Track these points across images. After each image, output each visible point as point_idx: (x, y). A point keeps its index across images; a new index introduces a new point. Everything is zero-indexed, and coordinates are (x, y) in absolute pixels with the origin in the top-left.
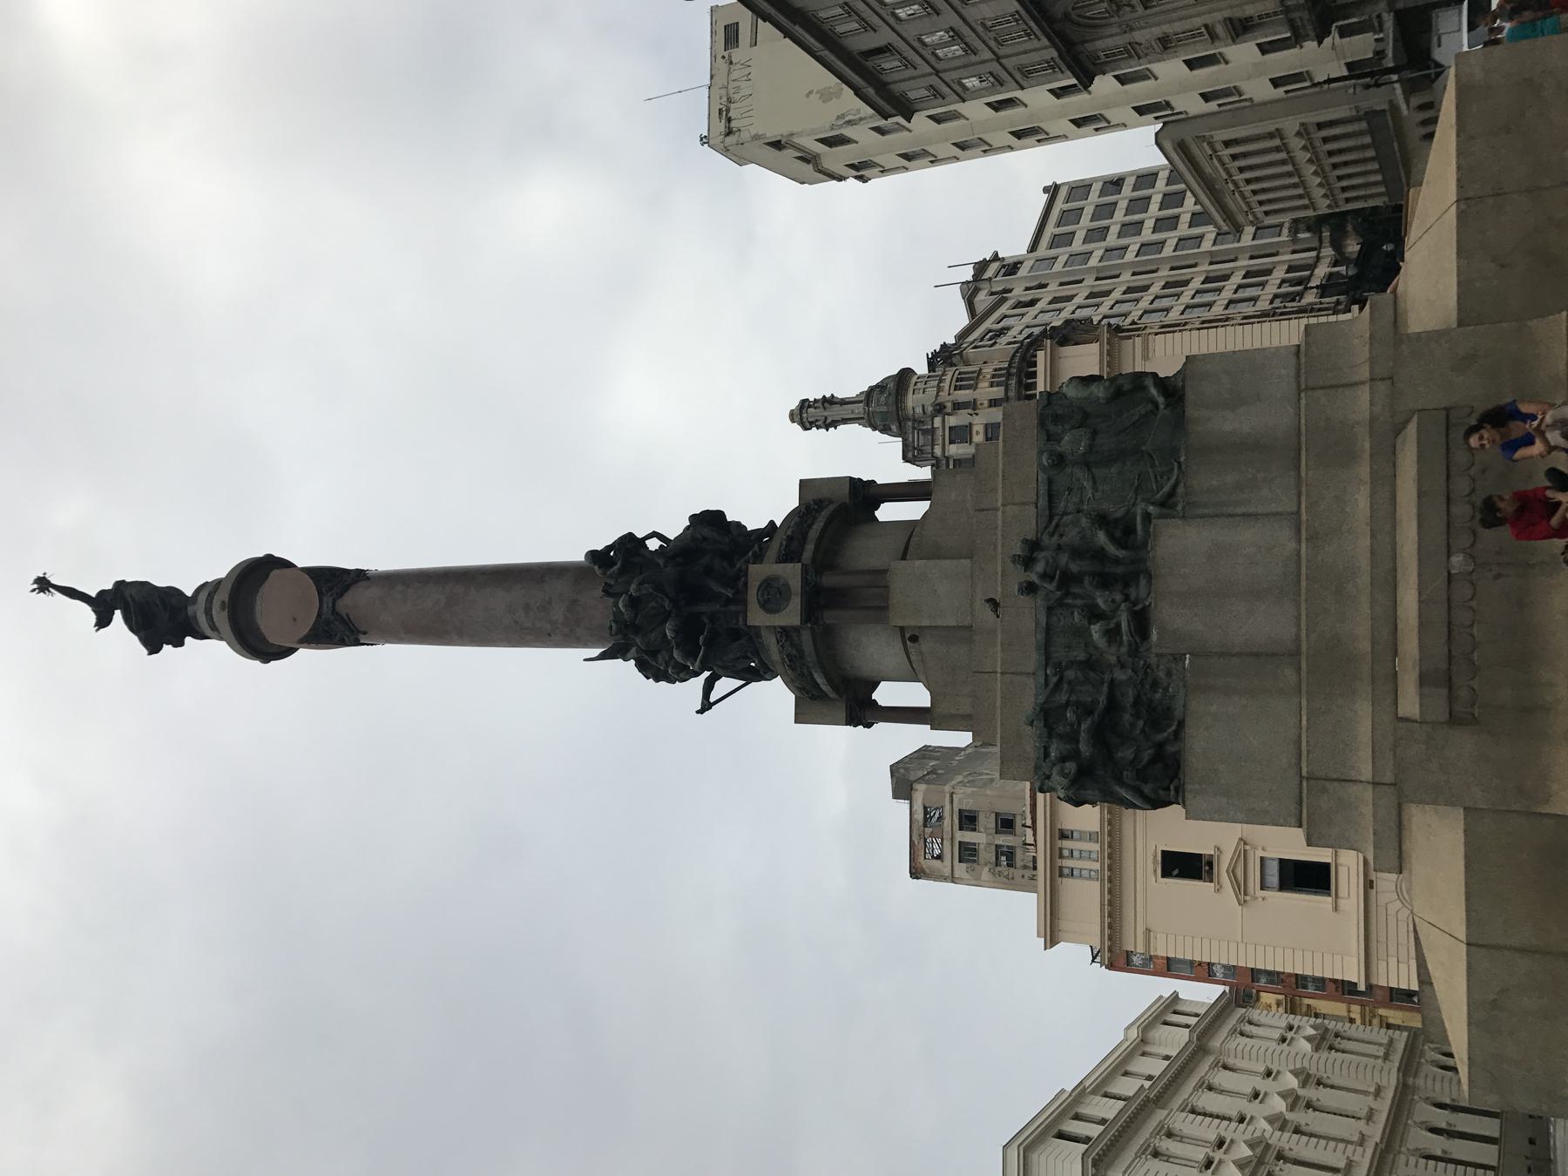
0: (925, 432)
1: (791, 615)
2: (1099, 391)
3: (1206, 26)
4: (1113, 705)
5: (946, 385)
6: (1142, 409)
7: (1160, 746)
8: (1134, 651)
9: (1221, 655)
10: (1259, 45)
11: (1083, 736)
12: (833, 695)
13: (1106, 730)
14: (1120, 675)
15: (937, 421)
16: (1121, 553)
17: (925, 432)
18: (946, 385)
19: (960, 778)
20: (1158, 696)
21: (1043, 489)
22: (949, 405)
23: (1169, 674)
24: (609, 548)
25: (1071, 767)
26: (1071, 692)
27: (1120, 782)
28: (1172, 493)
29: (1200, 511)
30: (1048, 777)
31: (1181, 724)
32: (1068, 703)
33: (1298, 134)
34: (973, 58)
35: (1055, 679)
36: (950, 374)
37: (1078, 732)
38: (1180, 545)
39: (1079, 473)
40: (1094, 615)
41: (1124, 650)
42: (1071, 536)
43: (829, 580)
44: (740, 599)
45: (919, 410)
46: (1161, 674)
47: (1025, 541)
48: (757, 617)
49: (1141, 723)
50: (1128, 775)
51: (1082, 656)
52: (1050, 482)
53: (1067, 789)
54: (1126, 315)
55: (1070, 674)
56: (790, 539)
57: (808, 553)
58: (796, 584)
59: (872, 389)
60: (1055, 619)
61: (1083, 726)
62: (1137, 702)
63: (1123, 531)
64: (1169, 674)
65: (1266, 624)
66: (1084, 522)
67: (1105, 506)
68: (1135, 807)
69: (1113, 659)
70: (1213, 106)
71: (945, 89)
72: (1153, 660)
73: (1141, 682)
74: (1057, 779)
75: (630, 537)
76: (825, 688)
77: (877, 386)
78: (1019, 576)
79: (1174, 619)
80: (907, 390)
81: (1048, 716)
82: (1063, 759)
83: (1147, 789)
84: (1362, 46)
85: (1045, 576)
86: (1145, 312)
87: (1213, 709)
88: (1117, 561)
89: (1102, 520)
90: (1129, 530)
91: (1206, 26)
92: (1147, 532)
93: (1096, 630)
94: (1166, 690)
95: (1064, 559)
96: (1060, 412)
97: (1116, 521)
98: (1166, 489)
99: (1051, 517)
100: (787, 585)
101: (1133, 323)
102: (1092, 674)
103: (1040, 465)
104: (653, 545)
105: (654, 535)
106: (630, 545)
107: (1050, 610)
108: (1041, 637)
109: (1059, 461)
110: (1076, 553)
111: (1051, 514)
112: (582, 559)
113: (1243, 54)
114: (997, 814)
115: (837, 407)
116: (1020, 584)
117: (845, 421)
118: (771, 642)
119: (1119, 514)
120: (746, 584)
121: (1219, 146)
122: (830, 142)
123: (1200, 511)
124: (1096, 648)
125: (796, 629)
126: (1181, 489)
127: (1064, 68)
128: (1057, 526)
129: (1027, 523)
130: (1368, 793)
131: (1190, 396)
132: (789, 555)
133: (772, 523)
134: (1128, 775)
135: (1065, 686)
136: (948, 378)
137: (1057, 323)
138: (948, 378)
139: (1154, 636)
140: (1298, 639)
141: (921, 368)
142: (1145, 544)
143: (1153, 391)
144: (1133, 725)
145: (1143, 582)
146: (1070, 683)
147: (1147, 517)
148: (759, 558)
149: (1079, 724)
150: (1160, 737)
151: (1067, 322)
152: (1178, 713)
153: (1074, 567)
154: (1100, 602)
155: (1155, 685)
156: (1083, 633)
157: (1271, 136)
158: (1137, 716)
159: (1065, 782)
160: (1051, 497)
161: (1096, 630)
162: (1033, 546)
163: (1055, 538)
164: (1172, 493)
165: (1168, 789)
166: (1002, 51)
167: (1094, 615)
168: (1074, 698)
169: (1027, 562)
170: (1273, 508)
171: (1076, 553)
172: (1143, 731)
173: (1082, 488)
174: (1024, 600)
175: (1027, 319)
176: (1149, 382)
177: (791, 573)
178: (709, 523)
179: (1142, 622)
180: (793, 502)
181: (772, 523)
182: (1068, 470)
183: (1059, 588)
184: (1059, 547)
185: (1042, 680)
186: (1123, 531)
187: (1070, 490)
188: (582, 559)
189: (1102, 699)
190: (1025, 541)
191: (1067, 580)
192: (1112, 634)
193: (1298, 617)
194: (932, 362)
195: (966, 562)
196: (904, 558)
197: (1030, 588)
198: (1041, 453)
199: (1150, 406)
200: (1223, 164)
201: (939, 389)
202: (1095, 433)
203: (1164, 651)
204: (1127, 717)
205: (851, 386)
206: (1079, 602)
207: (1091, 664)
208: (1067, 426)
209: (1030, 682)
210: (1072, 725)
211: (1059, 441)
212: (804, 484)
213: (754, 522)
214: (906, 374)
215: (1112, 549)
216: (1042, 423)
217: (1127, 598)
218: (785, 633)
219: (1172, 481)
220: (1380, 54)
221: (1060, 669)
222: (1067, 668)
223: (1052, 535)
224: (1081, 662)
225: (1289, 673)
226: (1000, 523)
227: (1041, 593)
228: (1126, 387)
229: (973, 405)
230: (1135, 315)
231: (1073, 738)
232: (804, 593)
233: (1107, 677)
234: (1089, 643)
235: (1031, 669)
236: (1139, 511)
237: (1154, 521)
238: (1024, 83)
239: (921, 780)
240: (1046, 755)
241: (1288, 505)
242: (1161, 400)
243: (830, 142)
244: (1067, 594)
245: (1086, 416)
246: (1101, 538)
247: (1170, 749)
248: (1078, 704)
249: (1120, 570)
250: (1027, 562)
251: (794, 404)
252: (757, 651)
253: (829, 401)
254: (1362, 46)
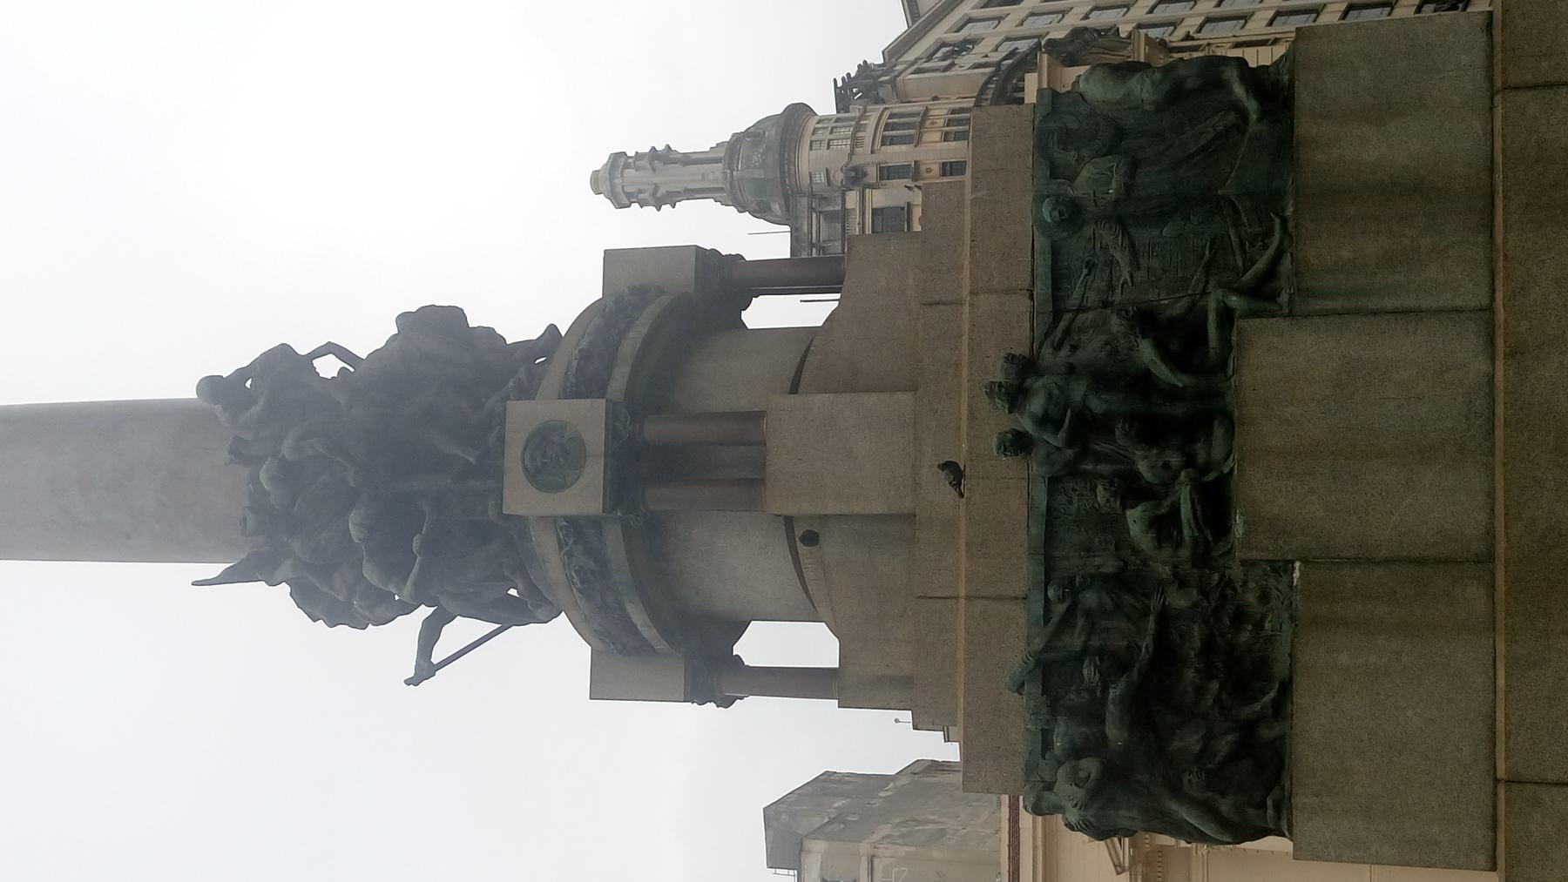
0: (831, 217)
1: (585, 495)
2: (1143, 89)
4: (1166, 654)
5: (867, 135)
6: (1219, 122)
7: (1248, 729)
8: (1203, 557)
9: (1356, 562)
11: (1112, 712)
12: (661, 645)
13: (1153, 702)
14: (1179, 601)
15: (852, 199)
16: (1180, 380)
17: (831, 217)
18: (867, 135)
19: (885, 829)
20: (1244, 637)
22: (873, 172)
23: (1264, 597)
24: (242, 374)
25: (1090, 767)
26: (1091, 630)
27: (1177, 792)
28: (1271, 273)
29: (1318, 305)
30: (1049, 787)
31: (1286, 688)
32: (1085, 651)
35: (1060, 609)
36: (874, 117)
37: (1103, 702)
38: (1283, 366)
39: (1107, 235)
40: (1131, 490)
41: (1185, 553)
42: (1092, 348)
43: (656, 430)
44: (490, 467)
45: (820, 179)
46: (1251, 598)
47: (1011, 358)
48: (522, 499)
49: (1214, 686)
51: (1110, 566)
52: (1055, 252)
53: (1085, 806)
54: (1174, 24)
56: (585, 356)
57: (618, 383)
58: (595, 438)
59: (738, 138)
60: (1062, 498)
61: (1114, 693)
62: (1208, 646)
63: (1183, 338)
64: (1264, 597)
66: (1116, 324)
67: (1152, 296)
68: (1202, 838)
69: (1165, 571)
72: (1236, 572)
73: (1216, 611)
74: (1065, 791)
75: (283, 353)
76: (649, 632)
77: (747, 133)
78: (999, 421)
80: (800, 140)
81: (1049, 674)
82: (1076, 753)
83: (1225, 806)
85: (1047, 421)
86: (1209, 20)
87: (1343, 658)
88: (1172, 394)
89: (1146, 321)
92: (1226, 346)
93: (1135, 519)
94: (1259, 626)
95: (1079, 390)
96: (1073, 126)
97: (1173, 322)
98: (1261, 265)
99: (1057, 315)
100: (578, 441)
101: (1188, 37)
102: (1128, 598)
103: (1039, 222)
104: (328, 367)
105: (330, 349)
106: (282, 368)
107: (1053, 483)
108: (1037, 530)
109: (1072, 215)
110: (1101, 379)
111: (1057, 312)
112: (191, 394)
115: (676, 169)
116: (1002, 436)
117: (691, 194)
118: (546, 544)
119: (1178, 309)
120: (502, 439)
123: (1318, 305)
124: (1136, 551)
125: (596, 523)
126: (1286, 265)
128: (1068, 331)
131: (1304, 97)
132: (583, 385)
133: (552, 329)
134: (1192, 781)
135: (1081, 622)
136: (870, 123)
137: (1059, 34)
138: (870, 123)
139: (1239, 529)
140: (1490, 533)
141: (825, 105)
142: (1223, 365)
143: (1239, 90)
144: (1200, 691)
145: (1218, 431)
146: (1088, 614)
148: (527, 391)
149: (1105, 689)
150: (1248, 711)
151: (1077, 33)
152: (1280, 668)
153: (1097, 405)
154: (1143, 467)
155: (1240, 617)
156: (1111, 524)
158: (1207, 673)
159: (1080, 794)
160: (1058, 278)
161: (1135, 519)
162: (1025, 368)
163: (1064, 352)
164: (1271, 273)
165: (1263, 806)
168: (1095, 642)
169: (1014, 395)
171: (1101, 379)
172: (1218, 700)
173: (1111, 263)
174: (1012, 466)
175: (1007, 27)
176: (1231, 74)
177: (588, 419)
178: (436, 333)
179: (1216, 502)
180: (592, 291)
181: (552, 329)
182: (1088, 230)
183: (1070, 443)
184: (1071, 370)
185: (1038, 609)
186: (1183, 338)
187: (1091, 266)
188: (191, 394)
189: (1146, 643)
190: (1011, 358)
192: (1165, 526)
193: (1491, 494)
194: (844, 93)
196: (794, 389)
197: (1018, 444)
198: (1039, 199)
199: (1232, 117)
201: (855, 142)
202: (1135, 165)
203: (1256, 555)
204: (1190, 675)
205: (702, 131)
206: (1104, 468)
207: (1128, 581)
208: (1085, 153)
209: (1018, 613)
210: (1092, 691)
211: (1071, 179)
212: (611, 258)
213: (519, 327)
214: (798, 113)
215: (1163, 372)
216: (1041, 147)
217: (1189, 462)
218: (575, 530)
219: (1271, 251)
221: (1072, 590)
222: (1084, 588)
223: (1058, 347)
224: (1106, 577)
225: (1474, 593)
226: (966, 327)
227: (1039, 453)
228: (1191, 84)
229: (912, 172)
230: (1191, 24)
231: (1094, 714)
233: (1155, 603)
234: (1122, 543)
235: (1020, 588)
236: (1212, 304)
237: (1239, 323)
239: (816, 833)
240: (1047, 745)
241: (1472, 295)
242: (1252, 106)
244: (1084, 453)
245: (1120, 134)
246: (1146, 352)
247: (1266, 733)
248: (1102, 652)
249: (1178, 409)
250: (1014, 395)
251: (600, 161)
252: (522, 565)
253: (662, 158)
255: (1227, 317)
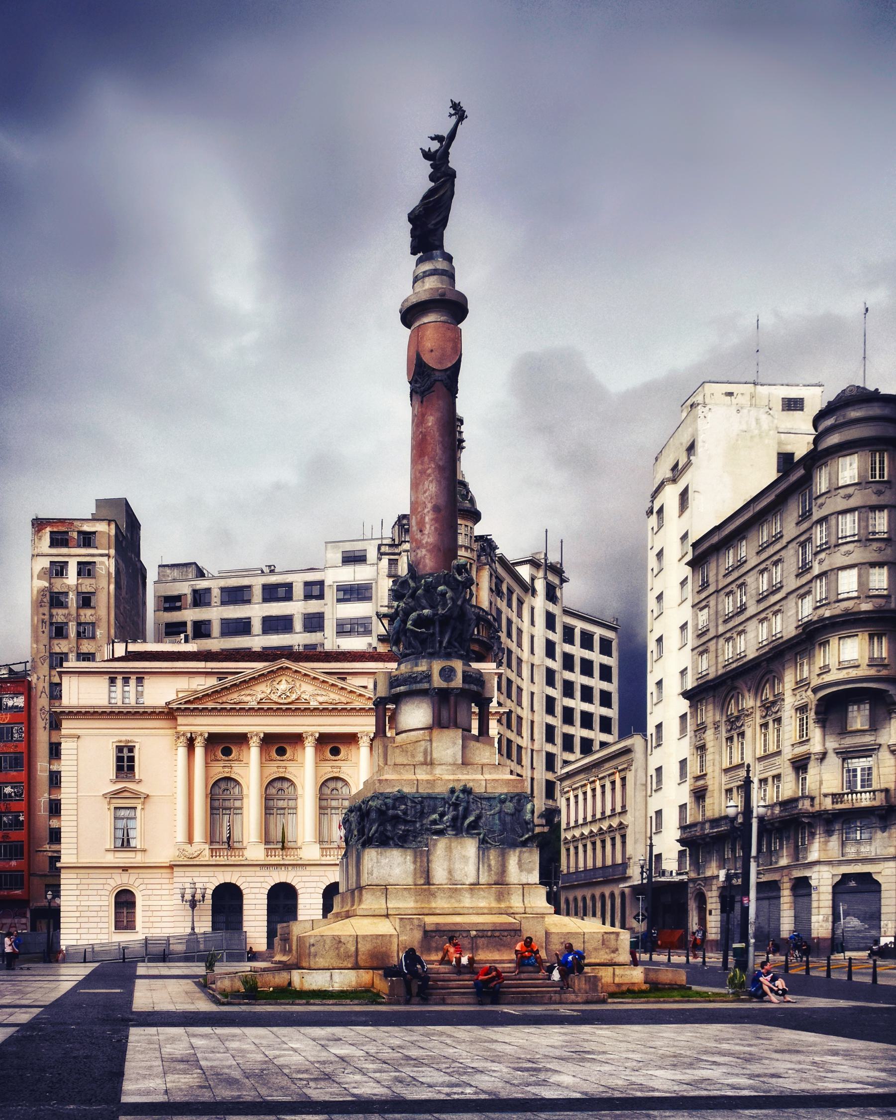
3: (705, 775)
6: (520, 831)
7: (392, 839)
8: (427, 829)
10: (686, 804)
21: (492, 795)
25: (384, 808)
27: (379, 826)
33: (621, 823)
34: (720, 621)
38: (469, 847)
50: (381, 828)
52: (495, 798)
55: (419, 807)
64: (420, 842)
65: (439, 874)
69: (424, 822)
70: (652, 771)
71: (703, 595)
82: (386, 804)
84: (670, 864)
88: (463, 823)
90: (475, 828)
91: (705, 775)
92: (472, 834)
93: (435, 816)
107: (444, 799)
109: (502, 802)
113: (684, 794)
114: (93, 593)
121: (623, 774)
122: (684, 496)
126: (489, 845)
127: (700, 682)
129: (479, 789)
134: (381, 828)
140: (433, 885)
147: (479, 834)
152: (406, 845)
153: (461, 808)
155: (415, 837)
156: (434, 812)
157: (624, 807)
158: (404, 831)
164: (487, 842)
167: (442, 815)
170: (481, 876)
179: (441, 833)
189: (409, 818)
192: (434, 822)
195: (460, 762)
200: (610, 775)
216: (518, 794)
220: (663, 873)
221: (421, 803)
225: (422, 882)
238: (696, 651)
240: (387, 798)
242: (523, 839)
243: (684, 496)
244: (450, 805)
246: (472, 818)
254: (670, 864)
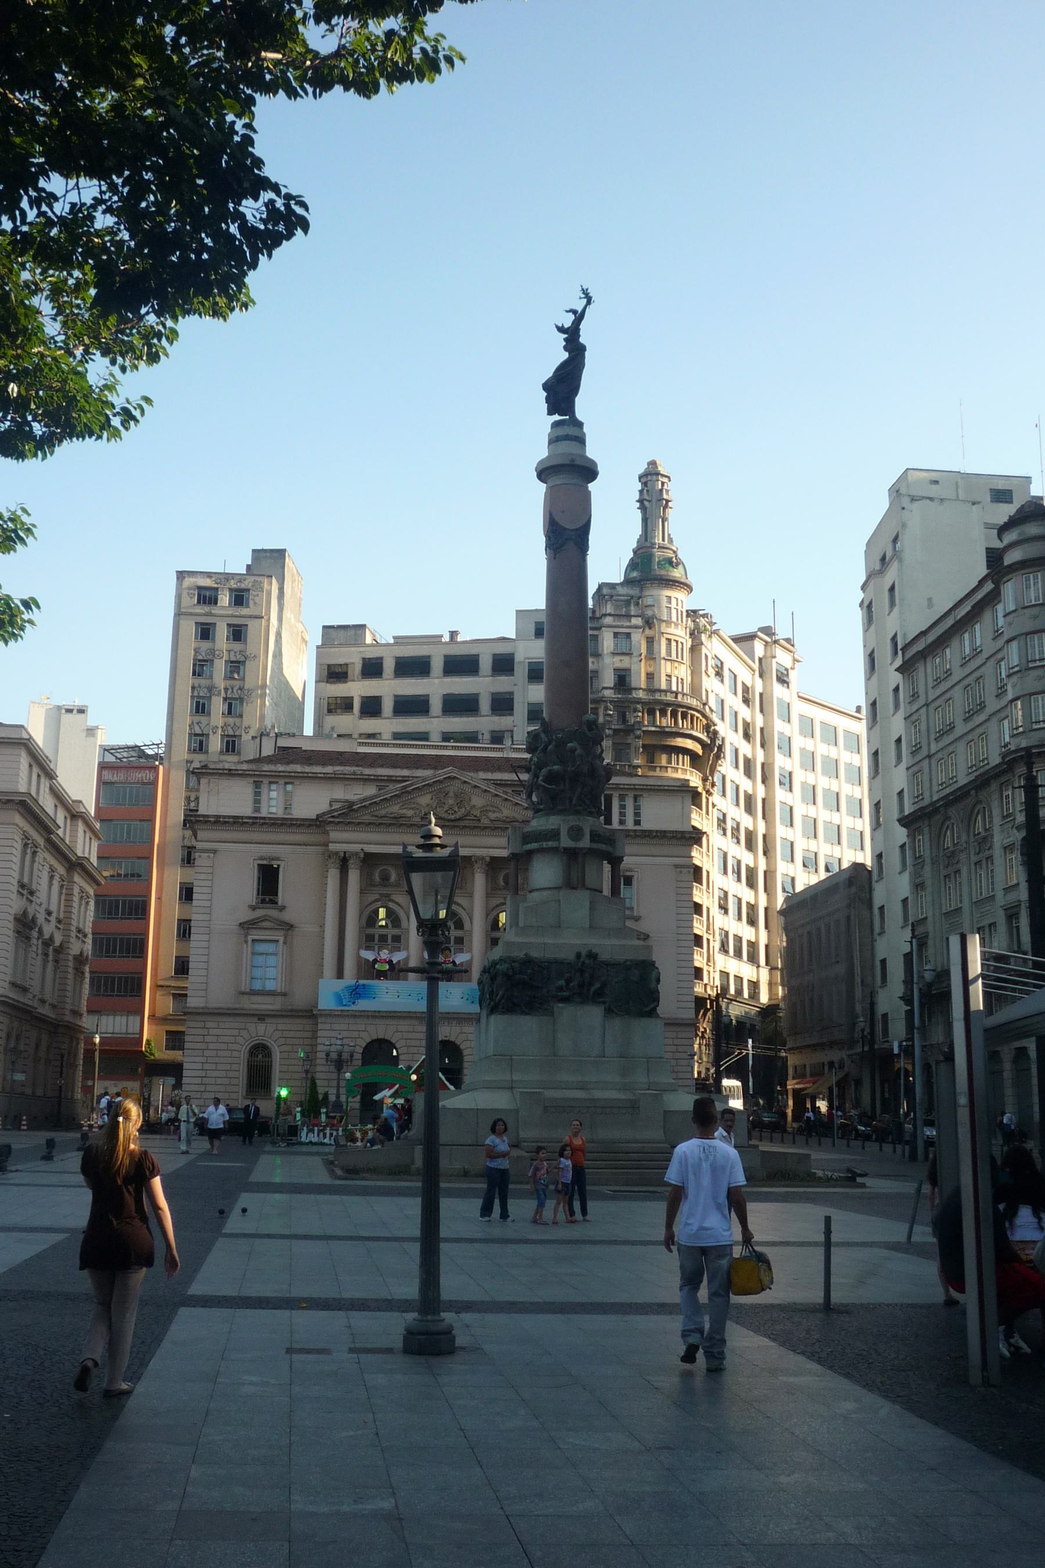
16: (591, 992)
38: (593, 1014)
79: (566, 1013)
89: (604, 985)
99: (607, 965)
111: (608, 964)
129: (604, 956)
130: (508, 1078)
153: (587, 975)
166: (934, 761)
186: (599, 994)
191: (582, 971)
215: (593, 989)
232: (574, 849)
246: (597, 985)
255: (604, 1003)
